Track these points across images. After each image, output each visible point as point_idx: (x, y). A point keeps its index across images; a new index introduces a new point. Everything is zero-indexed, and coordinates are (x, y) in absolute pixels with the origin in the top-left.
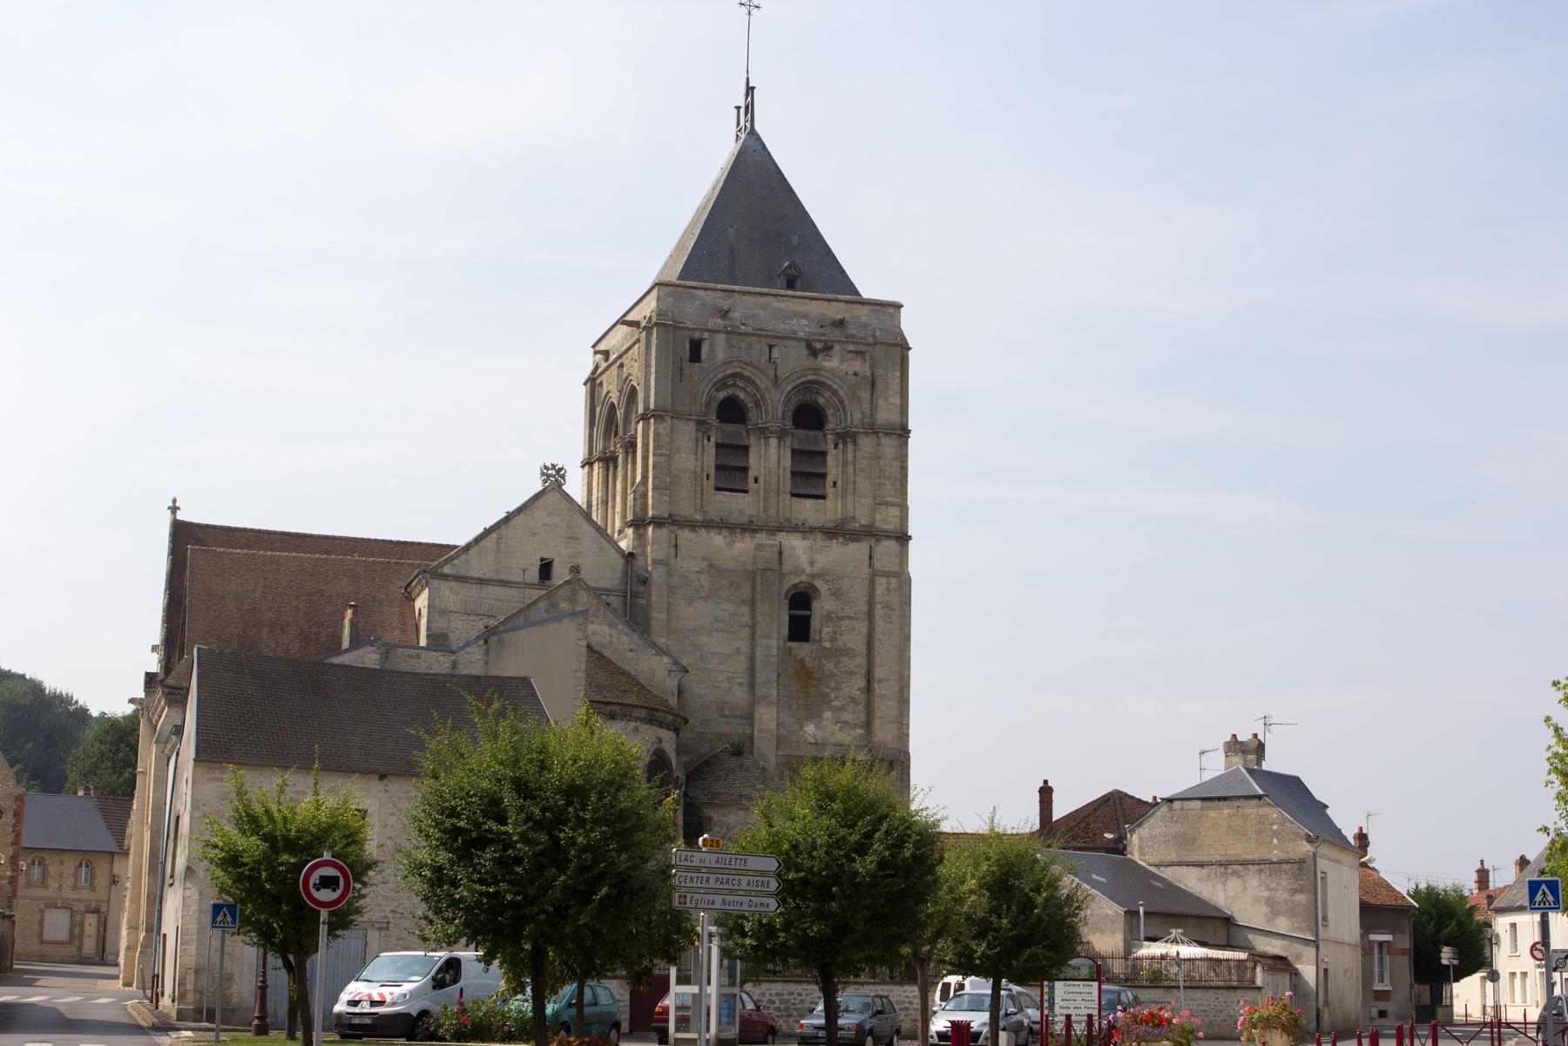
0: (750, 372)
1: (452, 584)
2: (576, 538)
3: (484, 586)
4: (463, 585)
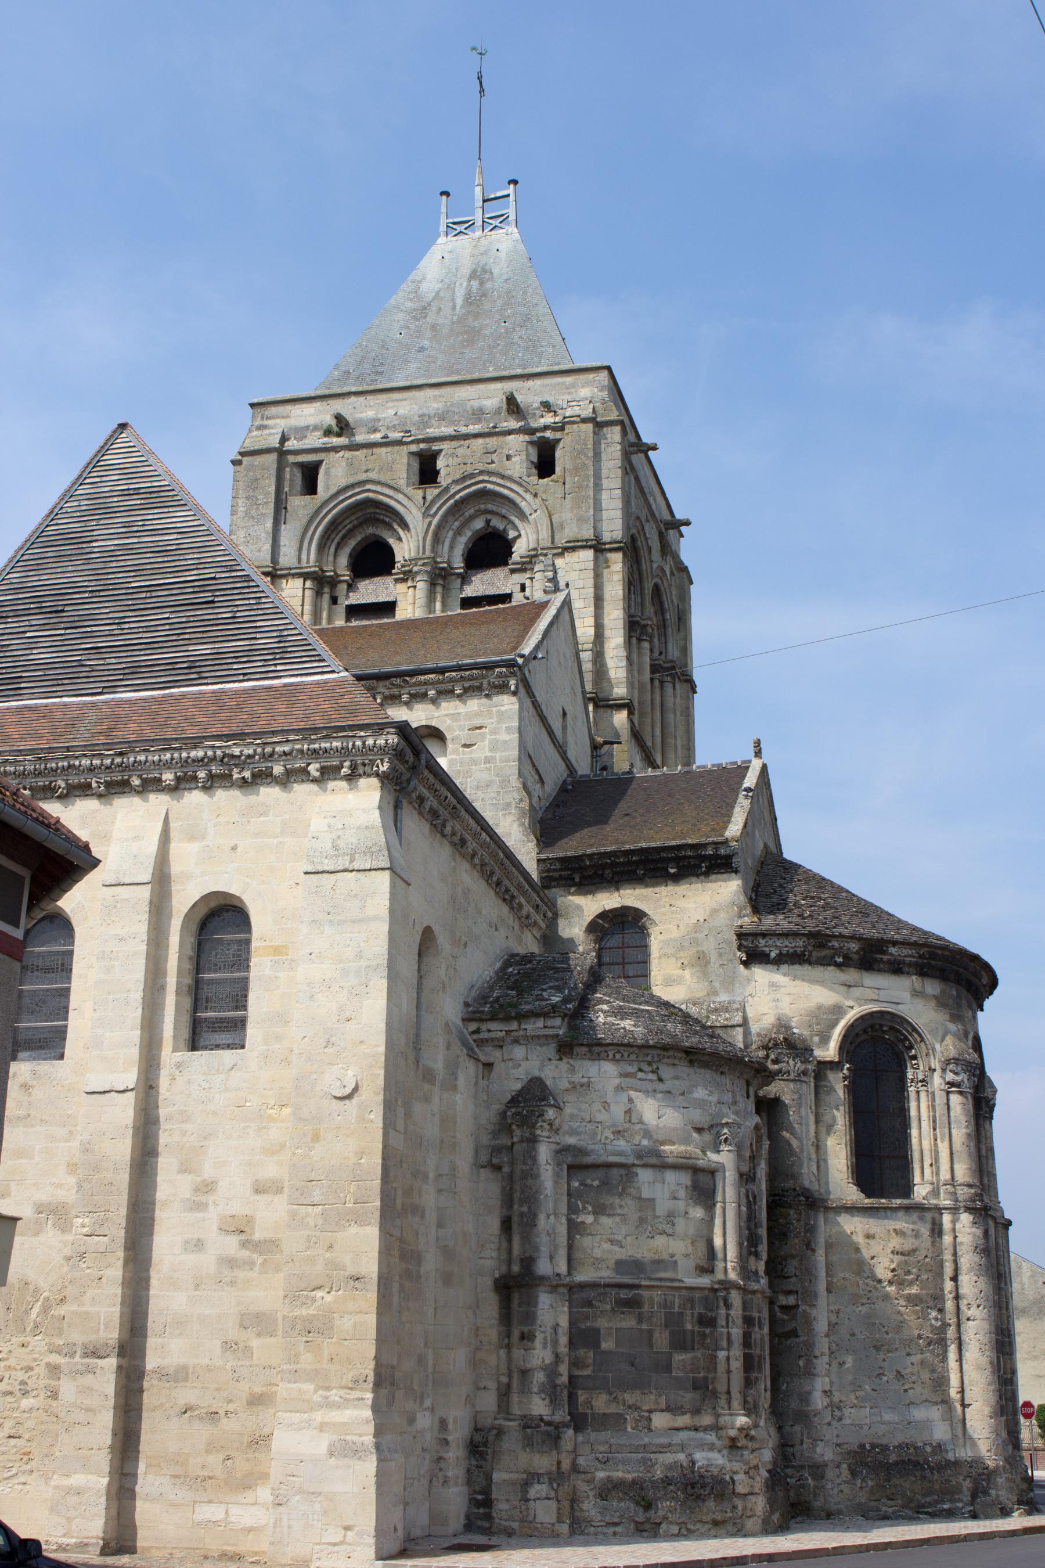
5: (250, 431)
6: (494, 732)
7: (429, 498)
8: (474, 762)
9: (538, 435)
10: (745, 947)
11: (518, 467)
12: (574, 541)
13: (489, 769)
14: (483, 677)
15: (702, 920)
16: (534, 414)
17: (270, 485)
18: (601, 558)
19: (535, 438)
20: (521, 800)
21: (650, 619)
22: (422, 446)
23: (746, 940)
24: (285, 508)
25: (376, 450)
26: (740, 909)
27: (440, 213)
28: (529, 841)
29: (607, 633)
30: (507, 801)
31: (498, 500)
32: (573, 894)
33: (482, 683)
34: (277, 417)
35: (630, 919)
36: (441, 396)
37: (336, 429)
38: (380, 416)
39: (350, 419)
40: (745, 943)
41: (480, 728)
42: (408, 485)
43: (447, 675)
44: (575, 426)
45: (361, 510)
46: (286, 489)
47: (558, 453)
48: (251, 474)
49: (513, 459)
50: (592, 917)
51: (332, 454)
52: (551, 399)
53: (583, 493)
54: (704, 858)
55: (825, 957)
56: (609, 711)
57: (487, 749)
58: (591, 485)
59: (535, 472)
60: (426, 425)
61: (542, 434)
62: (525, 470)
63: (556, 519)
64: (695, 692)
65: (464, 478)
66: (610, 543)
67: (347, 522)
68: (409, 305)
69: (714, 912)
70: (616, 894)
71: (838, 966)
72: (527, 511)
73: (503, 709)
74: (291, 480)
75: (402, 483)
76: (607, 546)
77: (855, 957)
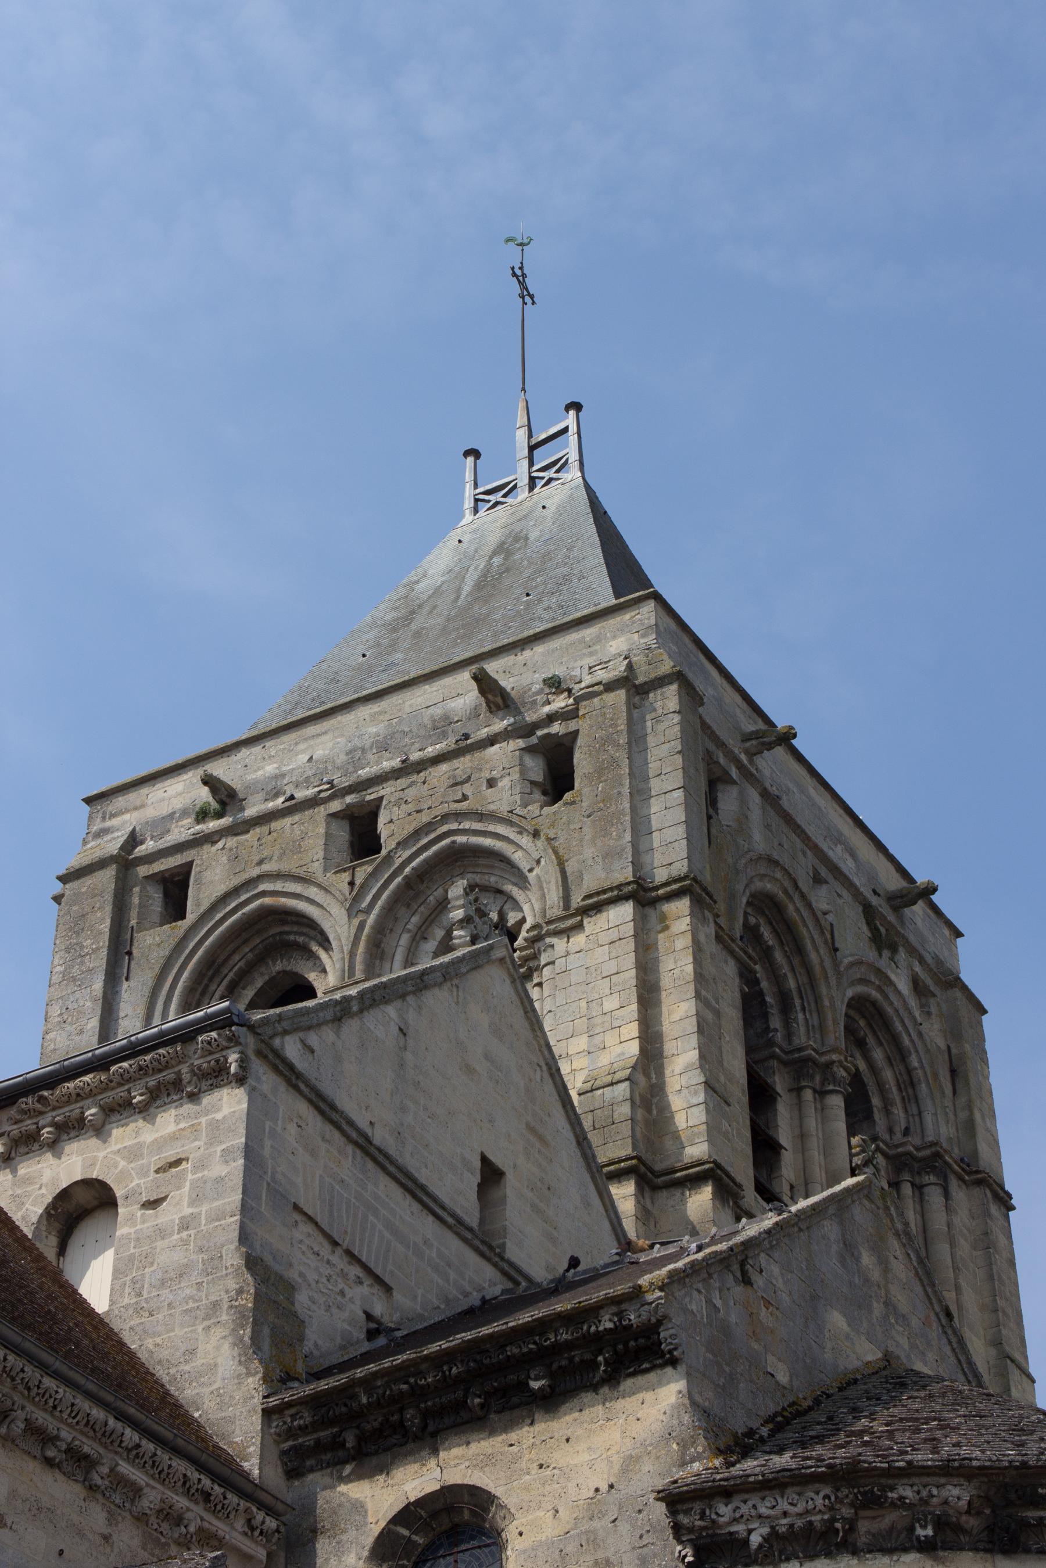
0: (797, 910)
1: (303, 1108)
2: (542, 1139)
3: (370, 1165)
4: (328, 1128)
5: (85, 842)
6: (200, 1166)
7: (358, 882)
8: (162, 1233)
9: (539, 733)
10: (691, 1530)
11: (506, 795)
12: (598, 893)
13: (185, 1243)
14: (181, 1059)
15: (604, 1487)
16: (534, 702)
17: (103, 919)
18: (652, 914)
19: (534, 740)
20: (240, 1292)
21: (835, 1050)
22: (349, 799)
23: (687, 1512)
24: (130, 953)
25: (275, 825)
26: (684, 1446)
27: (464, 483)
28: (249, 1374)
29: (669, 1047)
30: (213, 1298)
31: (482, 861)
32: (347, 1480)
33: (179, 1073)
34: (127, 811)
35: (466, 1516)
36: (383, 712)
37: (215, 805)
38: (284, 769)
39: (236, 785)
40: (684, 1520)
41: (178, 1162)
42: (326, 870)
43: (113, 1068)
44: (596, 700)
45: (259, 932)
46: (133, 922)
47: (578, 757)
48: (75, 908)
49: (500, 784)
50: (383, 1524)
51: (207, 847)
52: (560, 671)
53: (613, 808)
54: (597, 1340)
55: (892, 1529)
56: (677, 1193)
57: (185, 1203)
58: (626, 790)
59: (538, 795)
60: (358, 765)
61: (545, 731)
62: (518, 797)
63: (571, 867)
64: (1005, 1202)
65: (417, 834)
66: (666, 884)
67: (237, 957)
68: (389, 617)
69: (630, 1463)
70: (432, 1463)
71: (927, 1547)
72: (524, 866)
73: (219, 1116)
74: (141, 906)
75: (317, 868)
76: (661, 892)
77: (971, 1522)
